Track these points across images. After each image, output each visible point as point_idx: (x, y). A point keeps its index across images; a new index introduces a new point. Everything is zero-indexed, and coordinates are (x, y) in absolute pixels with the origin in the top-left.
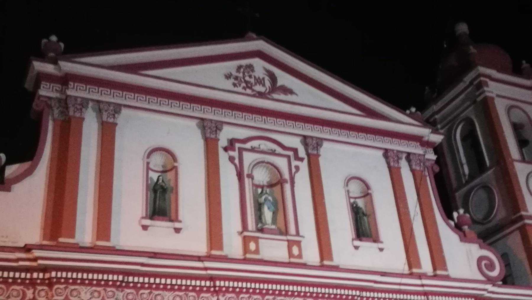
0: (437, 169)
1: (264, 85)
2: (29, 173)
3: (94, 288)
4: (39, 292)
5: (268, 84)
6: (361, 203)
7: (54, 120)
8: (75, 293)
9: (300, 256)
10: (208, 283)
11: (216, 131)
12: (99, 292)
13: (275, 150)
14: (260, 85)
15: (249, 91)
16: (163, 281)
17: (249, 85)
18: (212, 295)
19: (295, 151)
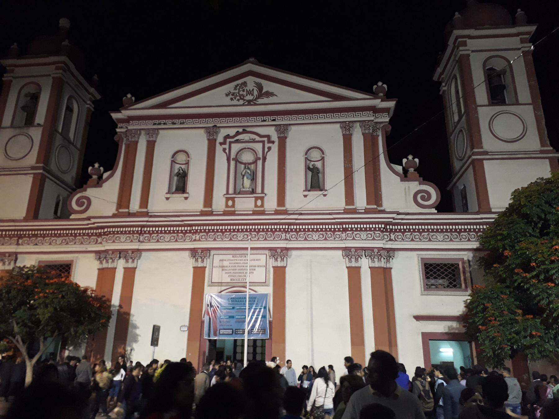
0: (389, 128)
1: (253, 95)
2: (111, 176)
3: (128, 235)
4: (104, 238)
5: (256, 93)
6: (319, 165)
7: (125, 144)
8: (118, 239)
9: (262, 206)
10: (189, 228)
11: (213, 134)
12: (130, 237)
13: (255, 139)
14: (249, 95)
15: (241, 102)
16: (157, 229)
17: (242, 97)
18: (193, 235)
19: (268, 137)
